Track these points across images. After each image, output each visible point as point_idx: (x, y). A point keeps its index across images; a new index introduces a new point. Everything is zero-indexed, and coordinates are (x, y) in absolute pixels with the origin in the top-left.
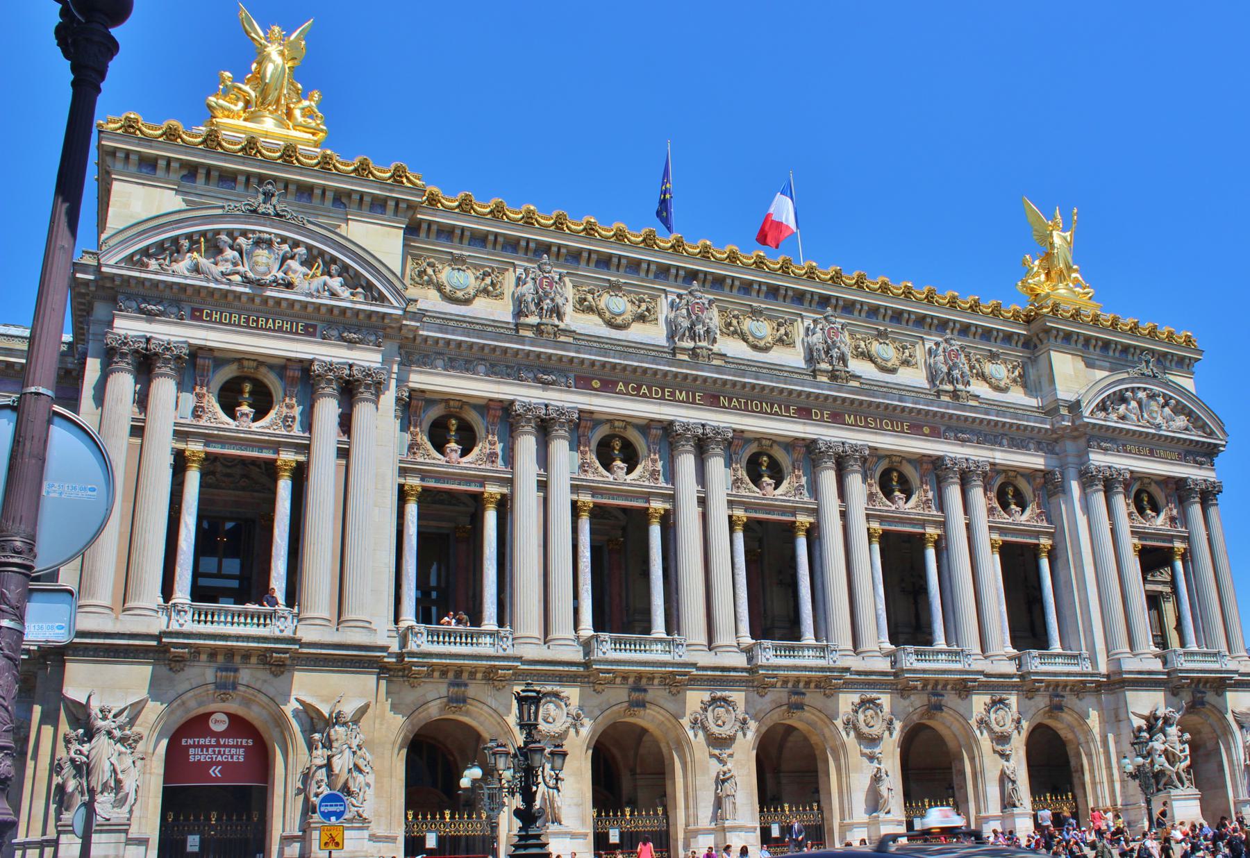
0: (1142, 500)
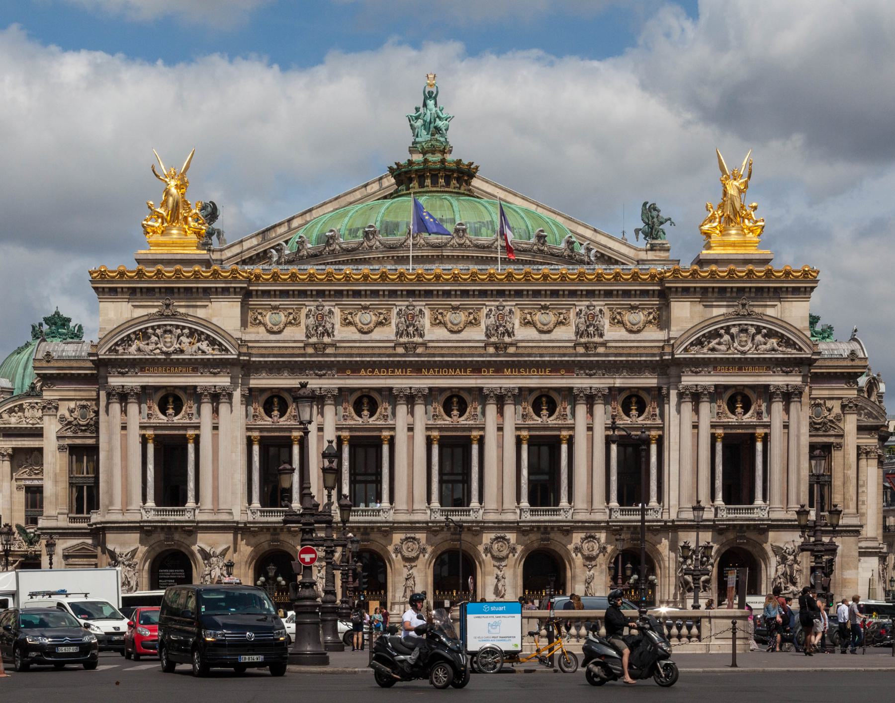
0: (736, 401)
